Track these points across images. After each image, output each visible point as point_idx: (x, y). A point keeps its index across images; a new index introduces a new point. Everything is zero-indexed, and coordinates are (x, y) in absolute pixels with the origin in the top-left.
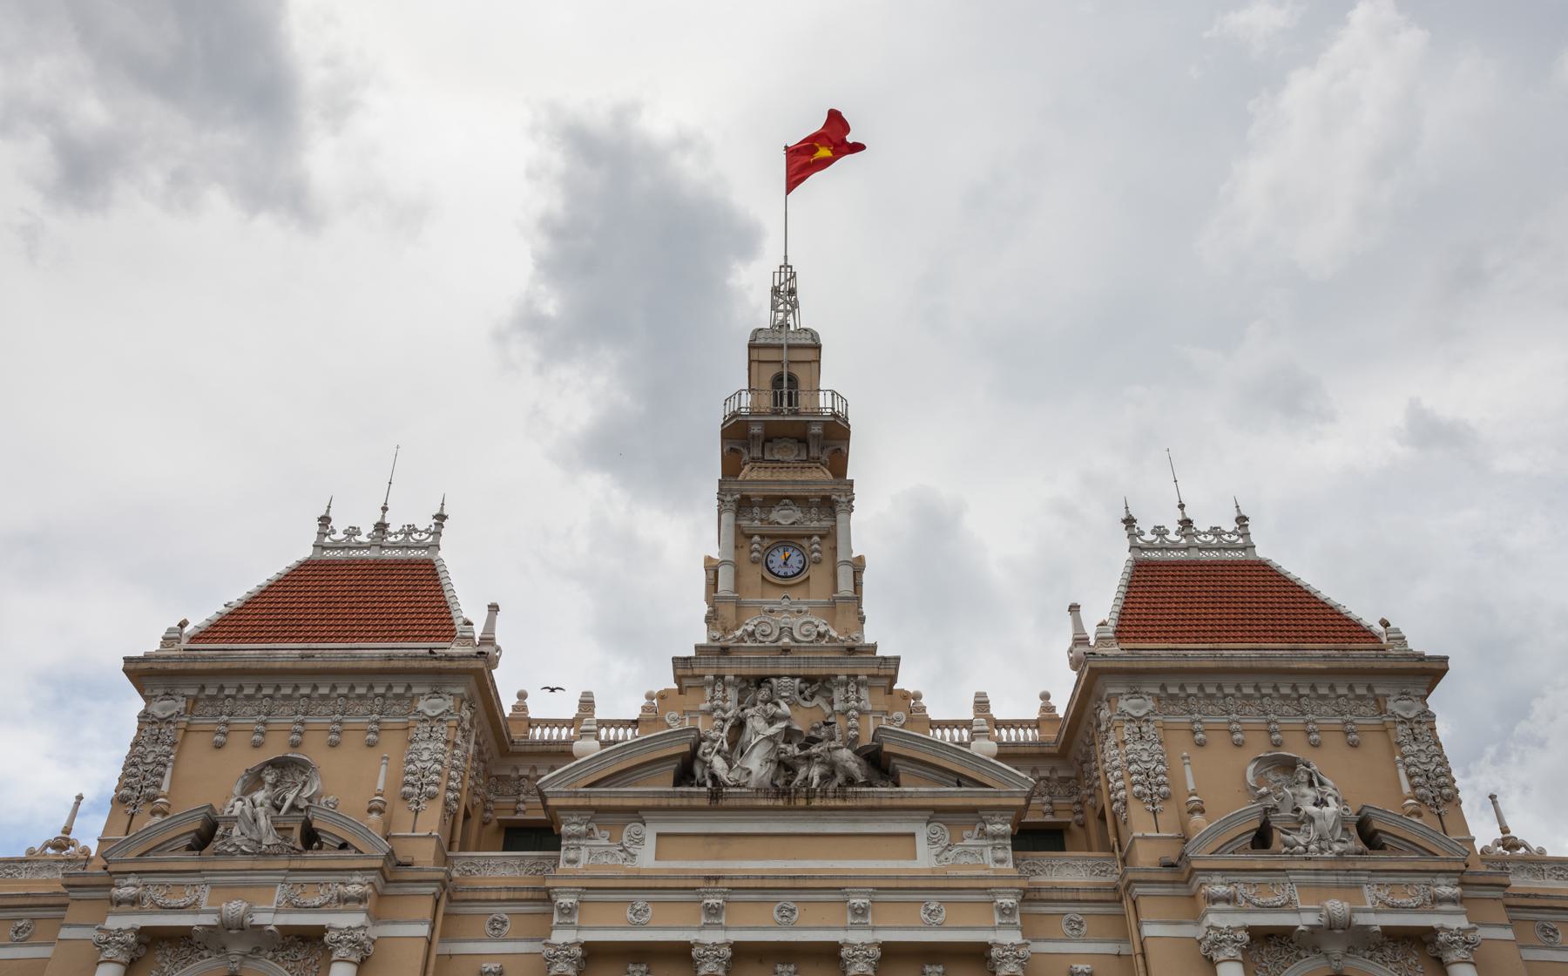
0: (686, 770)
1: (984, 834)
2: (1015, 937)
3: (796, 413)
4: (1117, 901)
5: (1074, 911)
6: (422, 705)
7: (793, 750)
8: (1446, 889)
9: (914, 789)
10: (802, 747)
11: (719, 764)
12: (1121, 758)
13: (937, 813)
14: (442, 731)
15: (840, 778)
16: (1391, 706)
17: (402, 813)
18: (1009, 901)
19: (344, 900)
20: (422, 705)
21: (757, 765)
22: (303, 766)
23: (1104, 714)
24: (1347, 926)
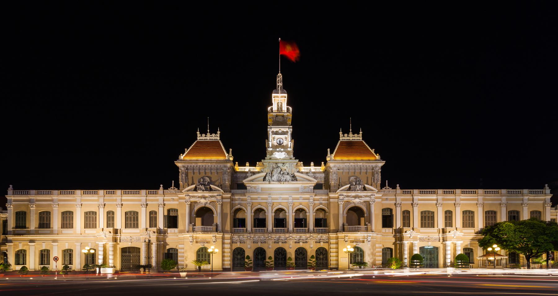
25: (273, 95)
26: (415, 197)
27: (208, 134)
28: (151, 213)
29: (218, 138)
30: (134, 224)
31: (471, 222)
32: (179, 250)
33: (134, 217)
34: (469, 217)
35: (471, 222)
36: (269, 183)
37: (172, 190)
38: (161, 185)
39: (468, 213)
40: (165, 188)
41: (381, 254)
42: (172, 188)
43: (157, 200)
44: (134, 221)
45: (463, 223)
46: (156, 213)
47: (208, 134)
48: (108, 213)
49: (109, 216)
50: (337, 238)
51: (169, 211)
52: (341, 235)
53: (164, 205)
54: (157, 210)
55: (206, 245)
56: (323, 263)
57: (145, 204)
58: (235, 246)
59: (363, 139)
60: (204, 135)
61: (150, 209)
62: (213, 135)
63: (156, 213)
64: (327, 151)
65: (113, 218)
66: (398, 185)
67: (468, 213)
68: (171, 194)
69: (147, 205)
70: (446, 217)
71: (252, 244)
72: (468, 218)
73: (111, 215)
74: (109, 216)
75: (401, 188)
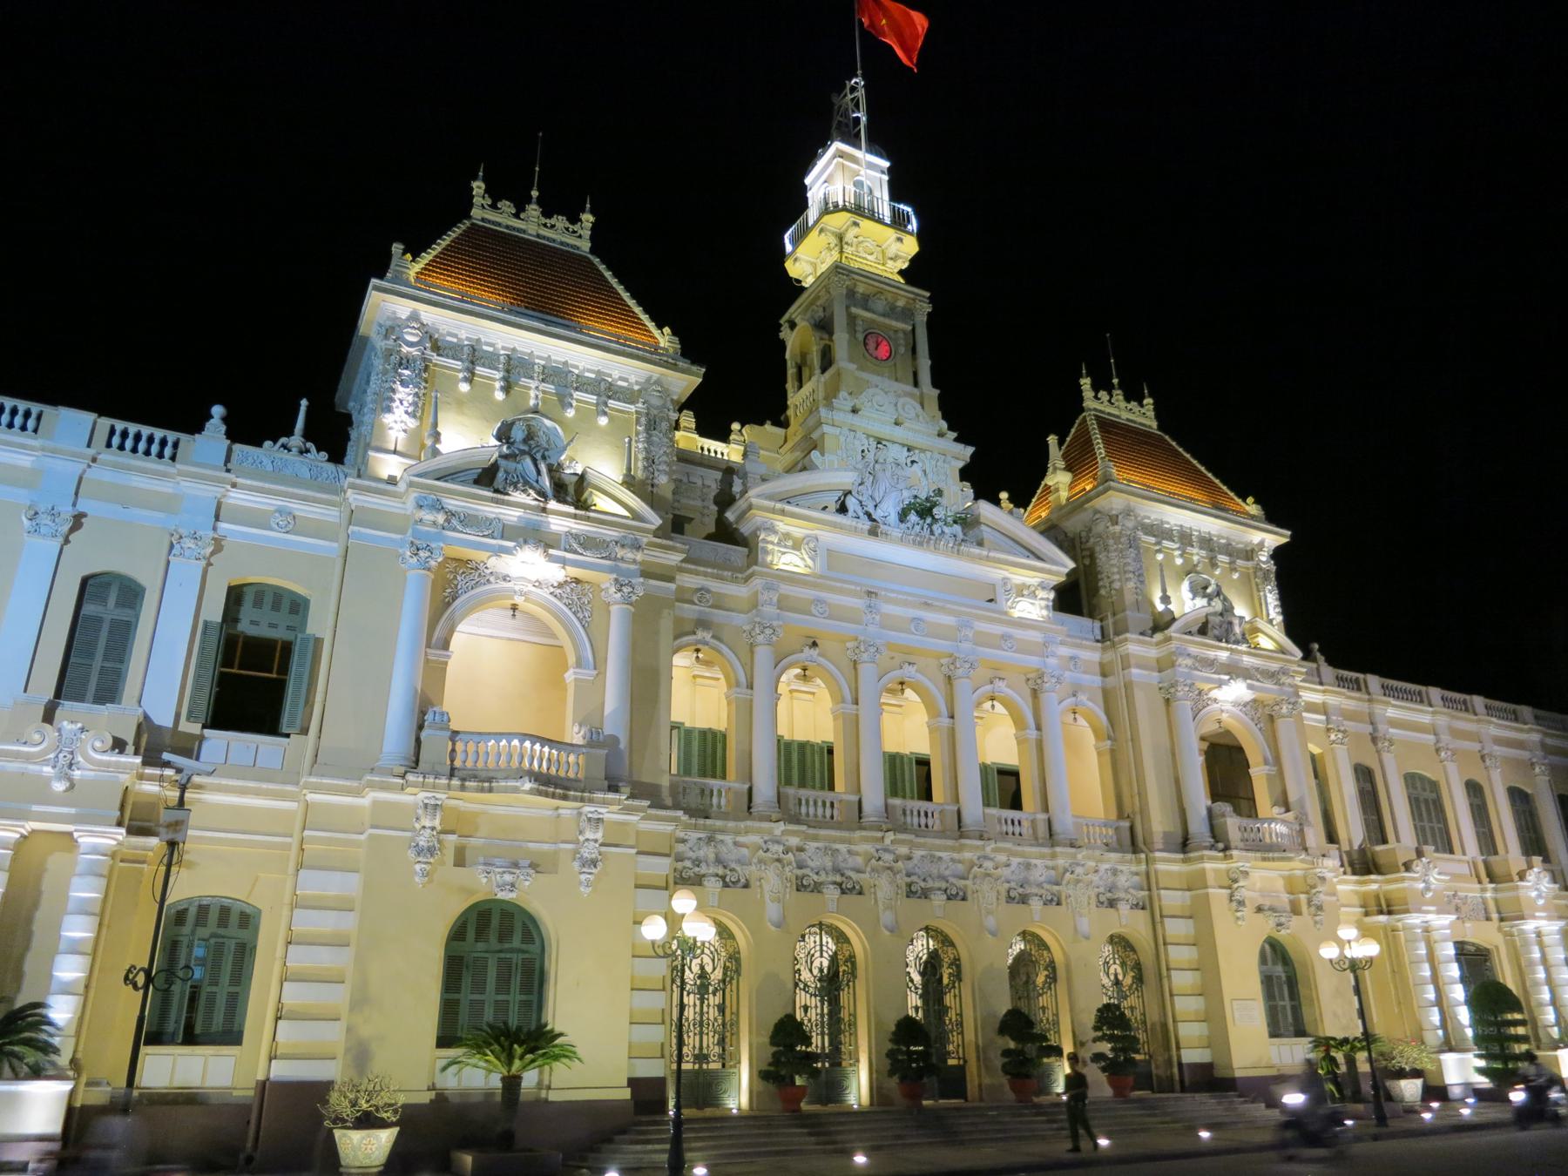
25: (837, 146)
26: (1378, 709)
27: (533, 210)
29: (585, 245)
36: (873, 532)
37: (292, 457)
38: (218, 411)
40: (245, 431)
42: (296, 440)
43: (167, 504)
46: (131, 593)
47: (533, 210)
50: (1196, 884)
51: (235, 596)
52: (1213, 865)
53: (218, 546)
54: (146, 577)
55: (529, 893)
57: (67, 512)
59: (1160, 428)
60: (506, 206)
61: (90, 556)
62: (560, 221)
63: (131, 593)
64: (1047, 445)
66: (1316, 646)
68: (277, 476)
69: (78, 521)
71: (791, 895)
75: (1332, 662)
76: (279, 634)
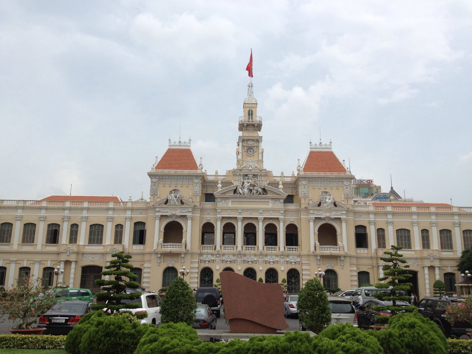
0: (235, 191)
1: (279, 202)
2: (283, 217)
3: (252, 121)
4: (298, 211)
5: (292, 213)
6: (194, 181)
7: (252, 188)
8: (344, 212)
9: (270, 195)
10: (253, 187)
11: (240, 190)
12: (302, 190)
13: (272, 199)
14: (198, 185)
15: (258, 193)
16: (345, 183)
17: (194, 198)
18: (282, 212)
19: (188, 211)
20: (194, 181)
21: (246, 190)
22: (178, 190)
23: (300, 183)
24: (329, 217)
28: (117, 226)
30: (98, 239)
31: (449, 242)
32: (144, 270)
33: (98, 232)
34: (447, 237)
35: (449, 242)
39: (445, 233)
41: (356, 278)
44: (98, 236)
45: (441, 244)
48: (73, 226)
49: (73, 229)
56: (295, 288)
58: (203, 265)
65: (77, 232)
67: (445, 233)
70: (423, 237)
72: (446, 238)
73: (75, 228)
74: (73, 229)
76: (142, 229)
